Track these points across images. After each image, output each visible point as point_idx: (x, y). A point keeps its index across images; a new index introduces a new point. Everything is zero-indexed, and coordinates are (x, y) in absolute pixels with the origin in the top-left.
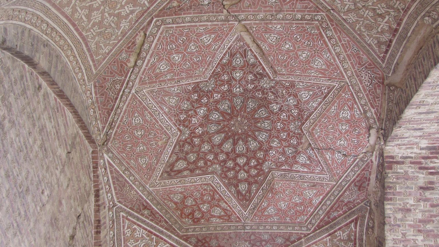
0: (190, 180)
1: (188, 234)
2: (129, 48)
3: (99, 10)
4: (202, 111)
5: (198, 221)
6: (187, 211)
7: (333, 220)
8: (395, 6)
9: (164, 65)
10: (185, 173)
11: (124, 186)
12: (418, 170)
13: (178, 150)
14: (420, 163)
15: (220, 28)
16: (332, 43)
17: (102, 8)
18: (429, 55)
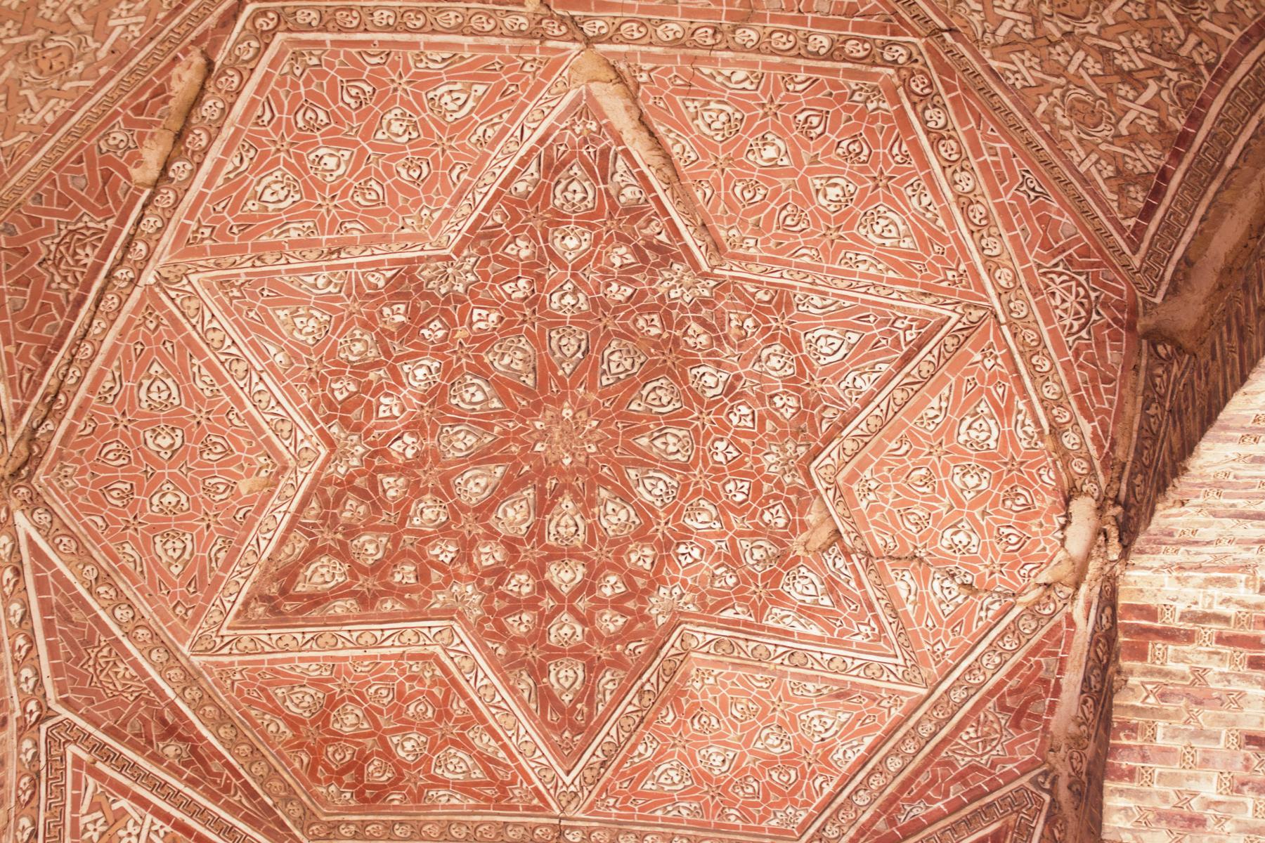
0: (355, 635)
2: (139, 109)
4: (420, 373)
6: (338, 756)
8: (1184, 52)
9: (277, 187)
10: (340, 607)
11: (88, 642)
12: (1245, 670)
13: (317, 516)
16: (945, 155)
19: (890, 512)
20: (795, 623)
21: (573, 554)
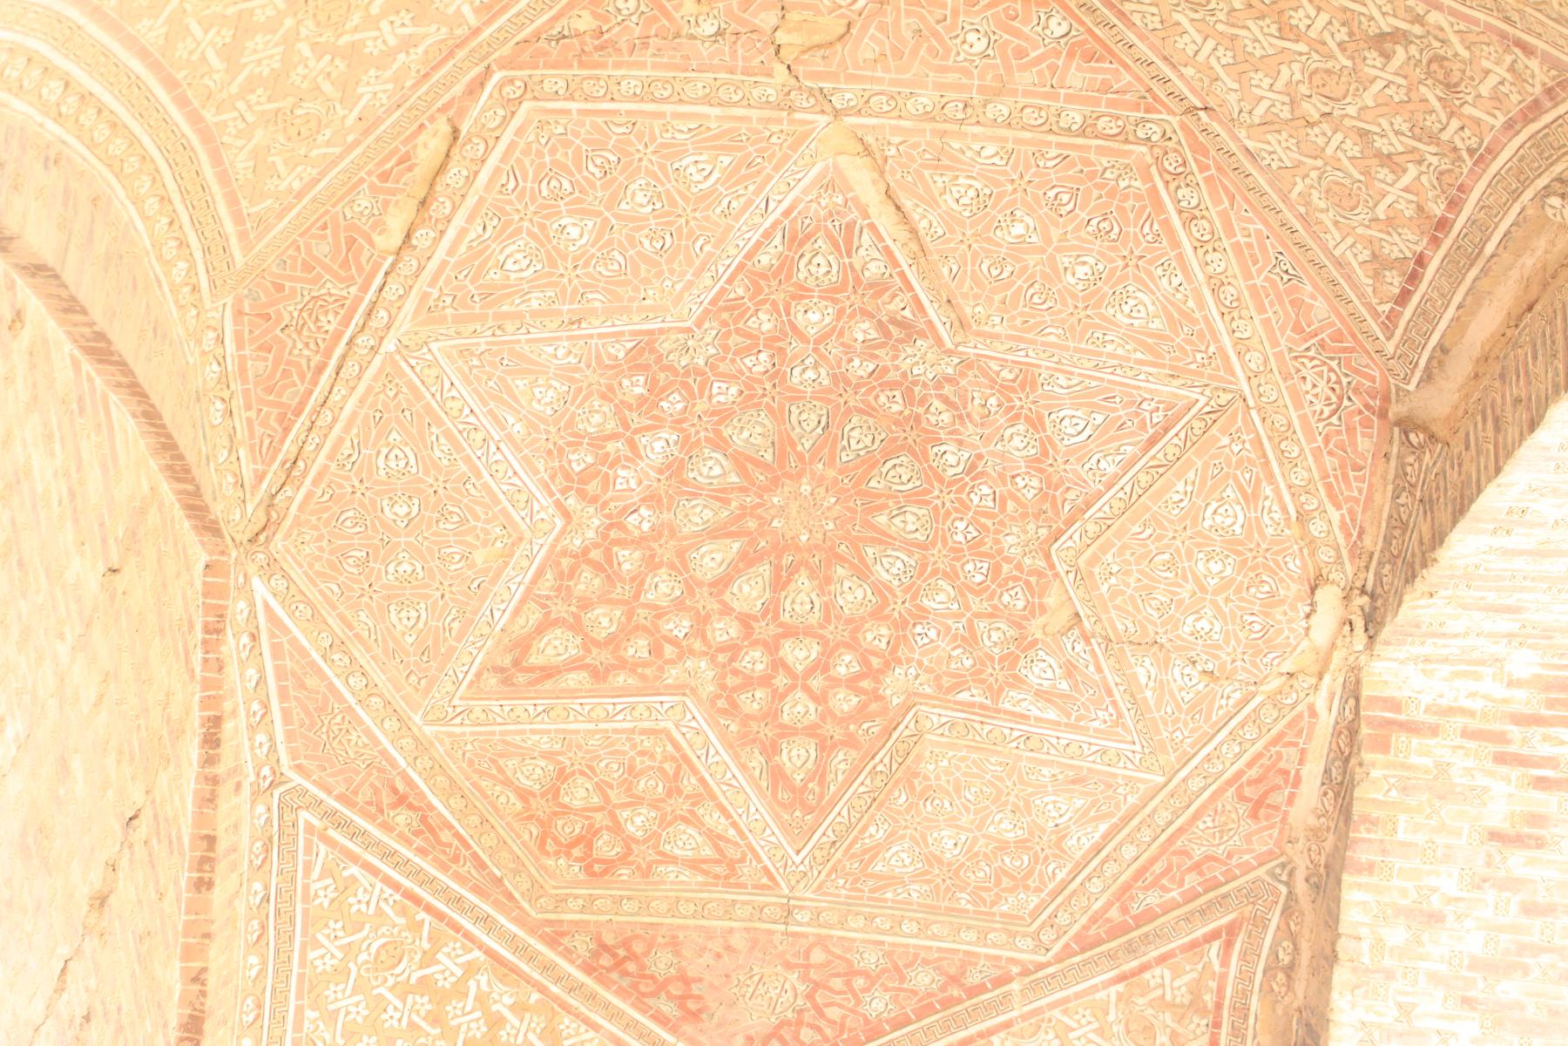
0: (587, 708)
1: (563, 917)
2: (385, 177)
3: (274, 32)
4: (658, 446)
5: (605, 872)
6: (566, 829)
7: (1140, 920)
8: (1445, 136)
9: (519, 256)
10: (573, 679)
12: (1490, 766)
13: (551, 589)
14: (1501, 738)
15: (757, 132)
16: (1198, 235)
17: (289, 22)
18: (1553, 342)
19: (1131, 596)
21: (808, 632)
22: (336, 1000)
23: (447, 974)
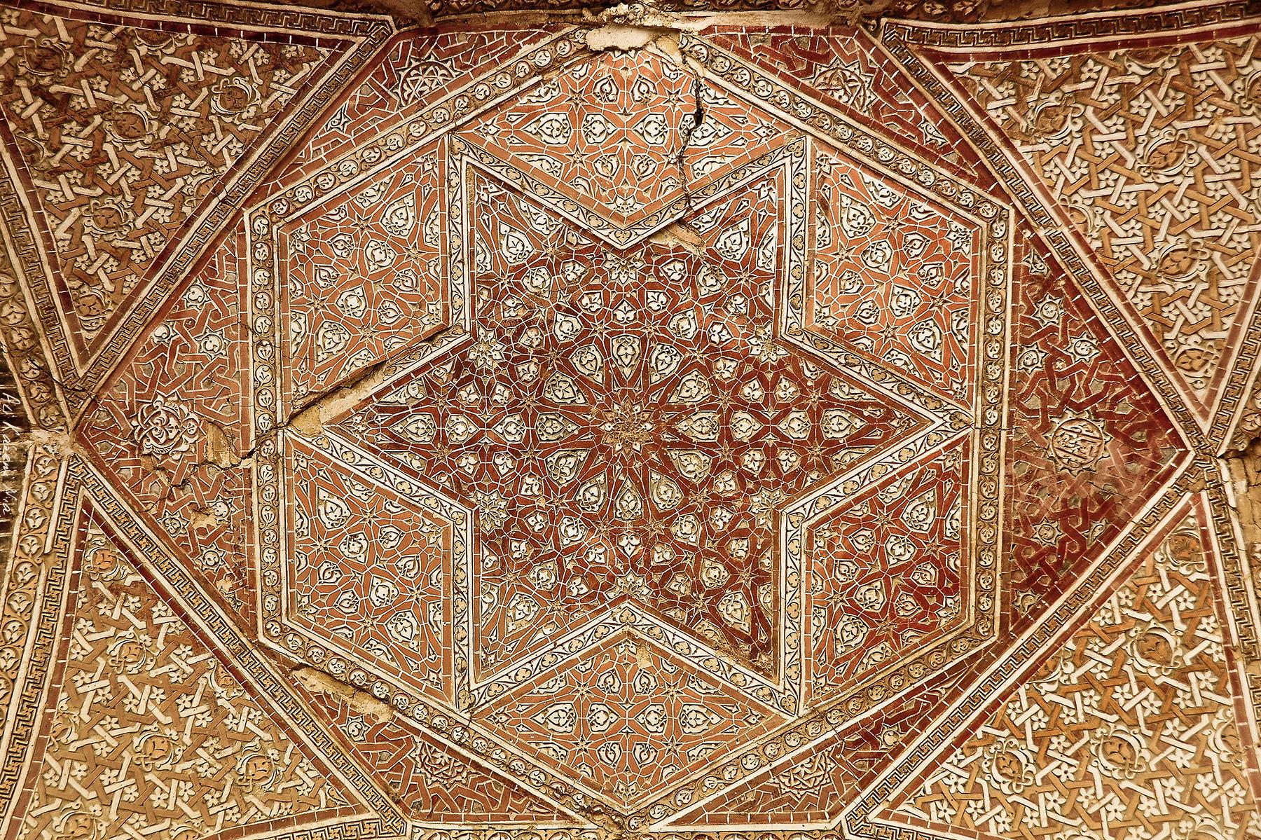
0: (789, 588)
1: (997, 614)
4: (571, 532)
5: (953, 578)
6: (908, 606)
9: (400, 627)
10: (765, 598)
11: (775, 792)
20: (769, 247)
21: (726, 421)
22: (1039, 818)
23: (1034, 718)
